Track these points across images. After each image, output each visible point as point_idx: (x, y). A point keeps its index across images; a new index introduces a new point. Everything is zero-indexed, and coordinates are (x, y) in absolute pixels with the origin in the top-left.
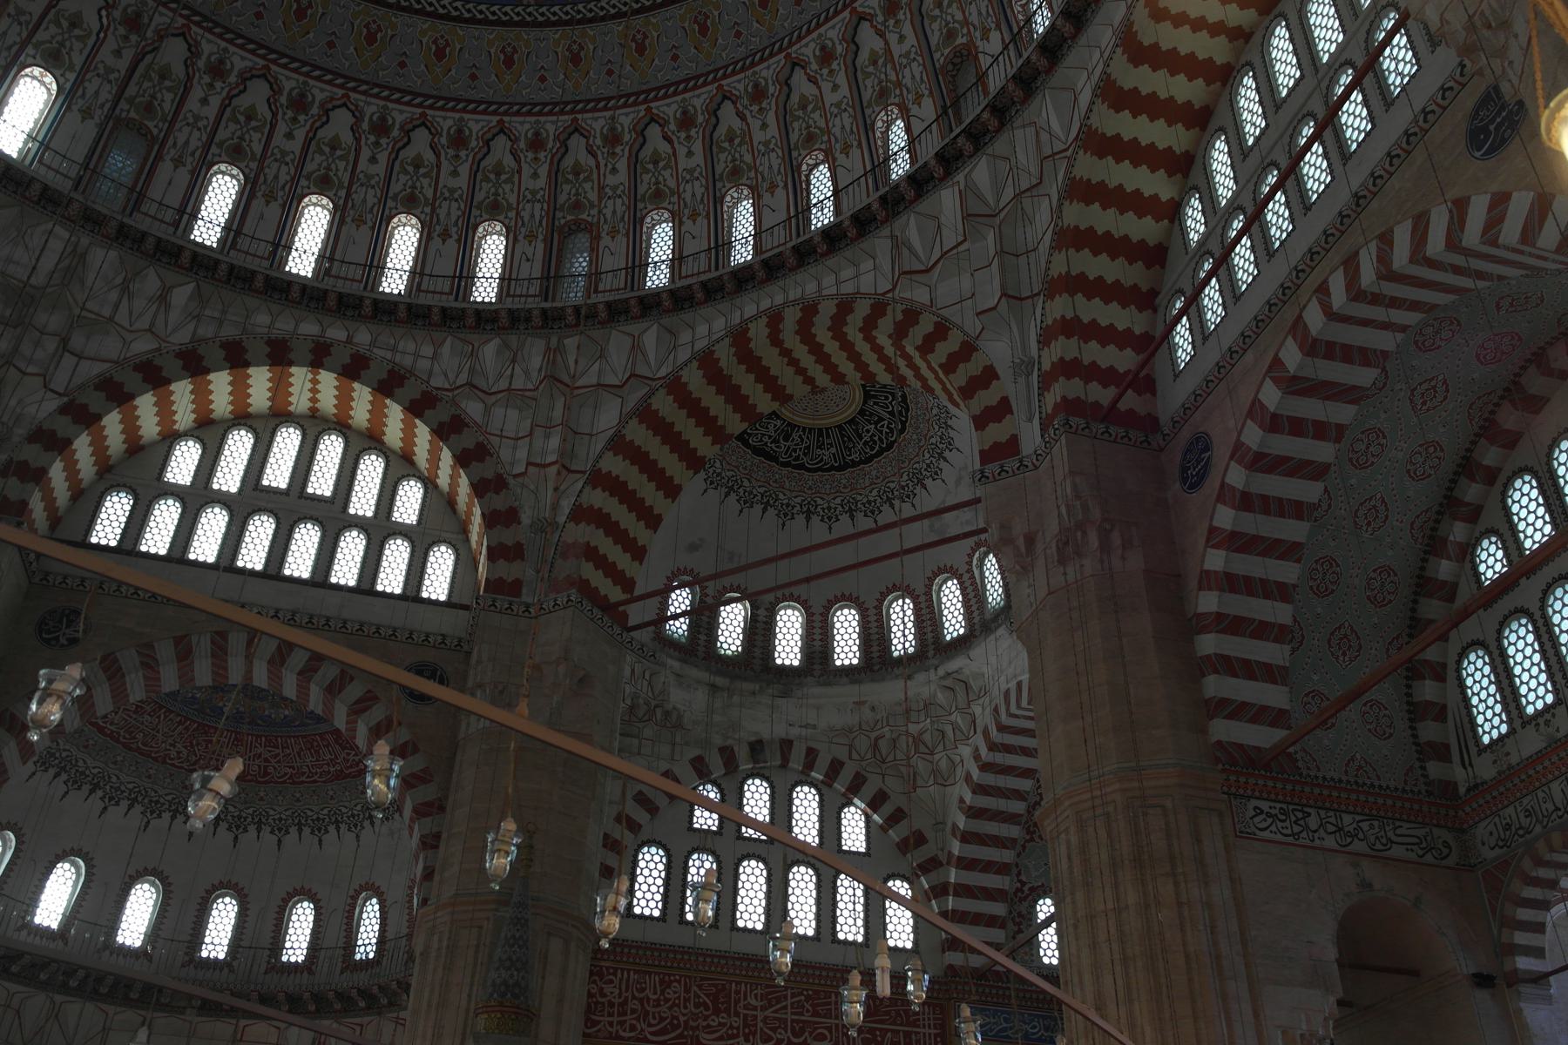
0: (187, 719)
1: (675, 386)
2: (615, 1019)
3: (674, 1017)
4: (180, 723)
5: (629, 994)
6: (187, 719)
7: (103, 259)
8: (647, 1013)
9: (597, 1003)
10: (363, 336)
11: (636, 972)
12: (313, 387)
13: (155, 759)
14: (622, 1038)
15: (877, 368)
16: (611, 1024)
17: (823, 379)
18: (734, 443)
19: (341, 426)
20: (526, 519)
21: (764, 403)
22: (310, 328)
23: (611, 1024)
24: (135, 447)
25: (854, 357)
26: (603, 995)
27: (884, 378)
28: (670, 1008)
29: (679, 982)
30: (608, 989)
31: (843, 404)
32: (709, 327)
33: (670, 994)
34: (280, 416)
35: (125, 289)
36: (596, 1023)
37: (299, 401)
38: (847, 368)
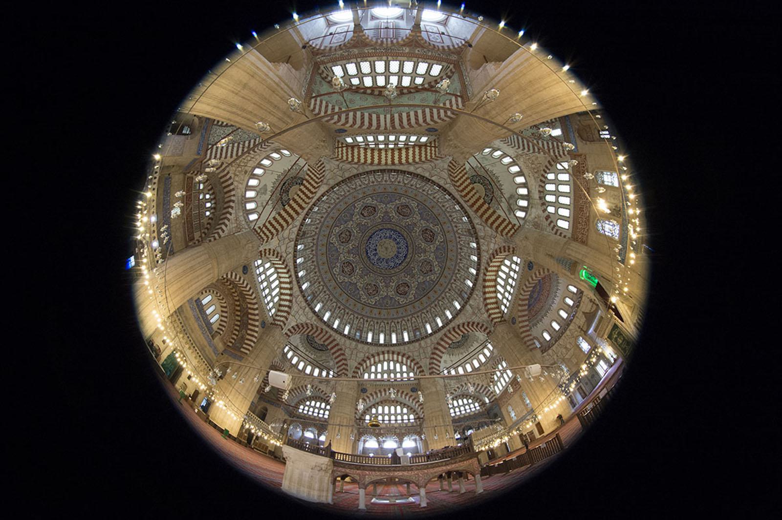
1: (481, 216)
7: (471, 302)
10: (482, 267)
12: (490, 276)
15: (466, 183)
17: (474, 191)
18: (490, 205)
19: (497, 271)
20: (504, 245)
21: (481, 201)
22: (482, 275)
24: (496, 303)
25: (466, 187)
27: (469, 181)
31: (478, 186)
32: (471, 212)
34: (495, 280)
35: (475, 299)
37: (494, 277)
38: (469, 188)
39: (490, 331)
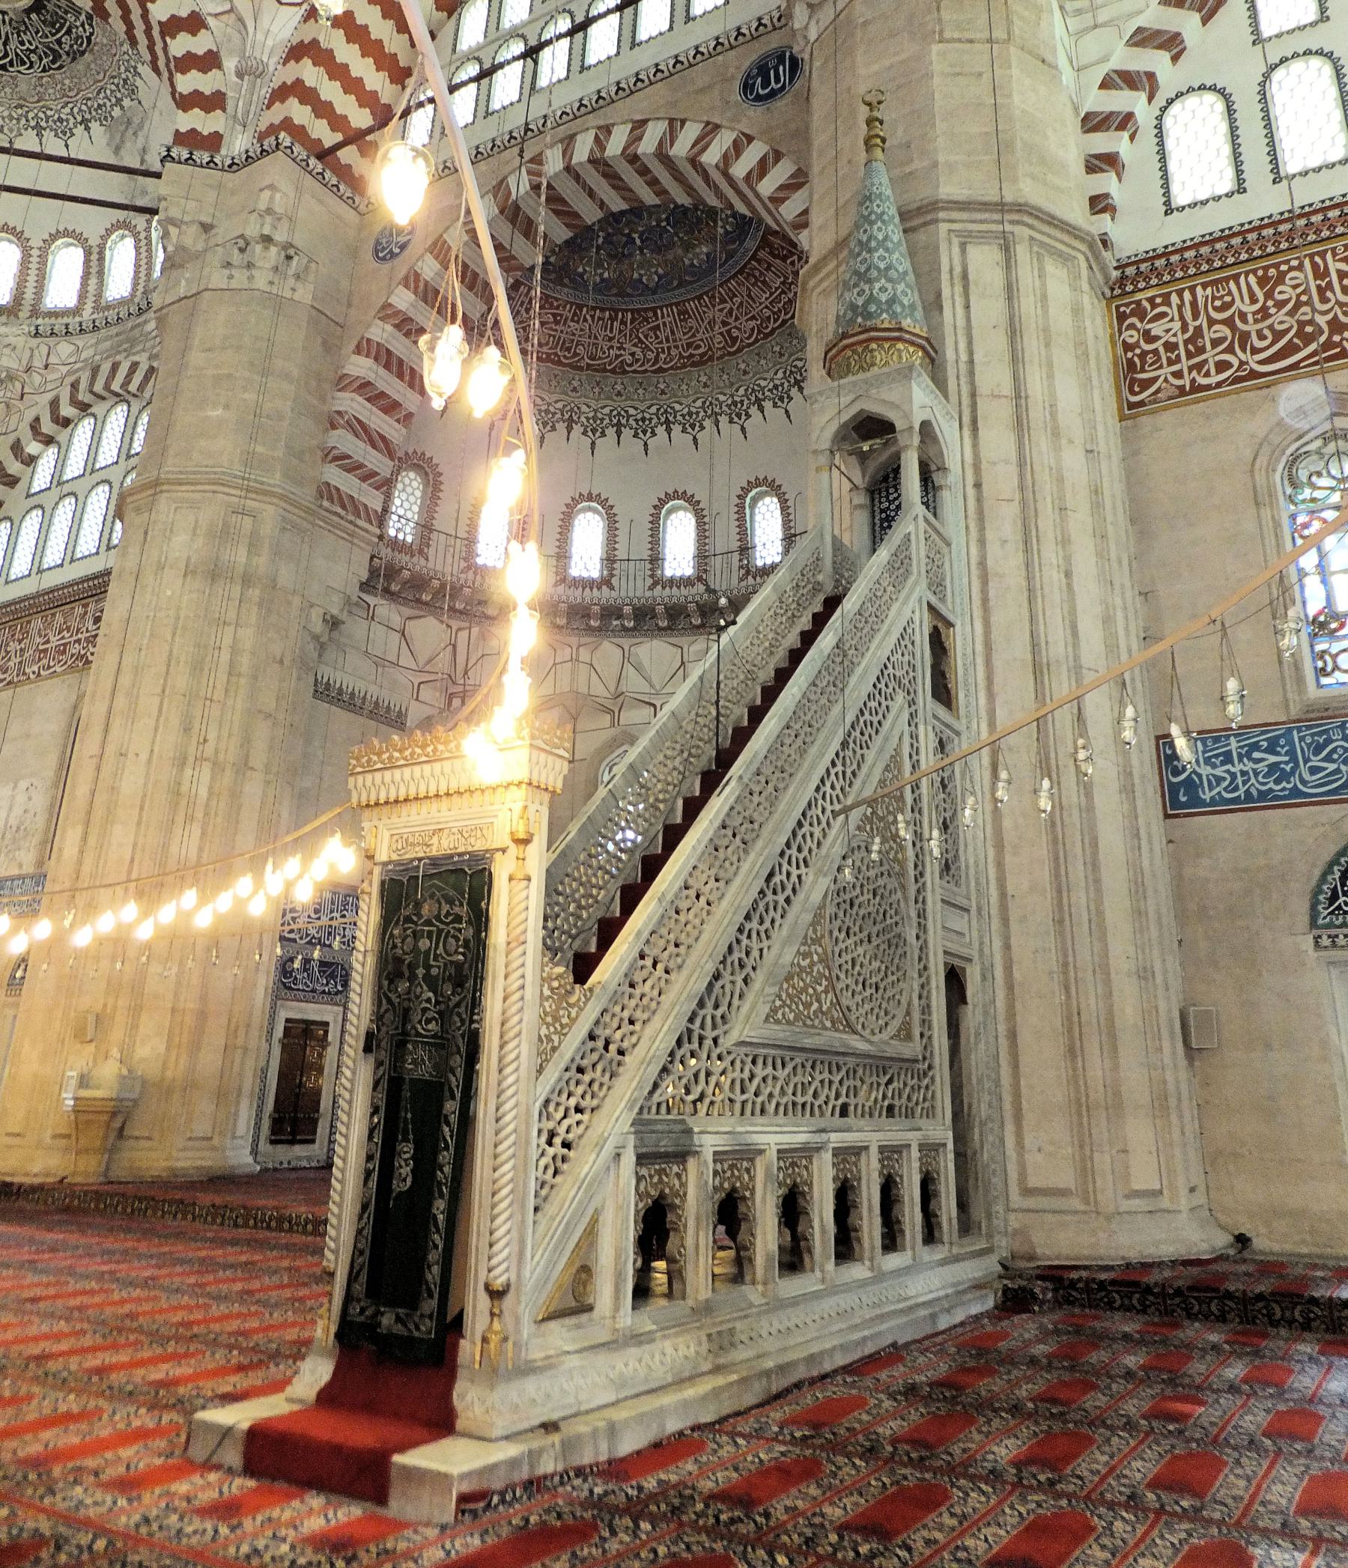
0: (616, 311)
2: (1184, 364)
3: (1302, 324)
4: (612, 319)
5: (1202, 320)
6: (616, 311)
8: (1244, 337)
9: (1143, 355)
11: (1204, 286)
13: (613, 371)
14: (1208, 387)
16: (1178, 375)
23: (1178, 375)
26: (1150, 338)
28: (1291, 313)
29: (1300, 267)
30: (1157, 328)
33: (1285, 291)
36: (1146, 384)
39: (214, 141)
